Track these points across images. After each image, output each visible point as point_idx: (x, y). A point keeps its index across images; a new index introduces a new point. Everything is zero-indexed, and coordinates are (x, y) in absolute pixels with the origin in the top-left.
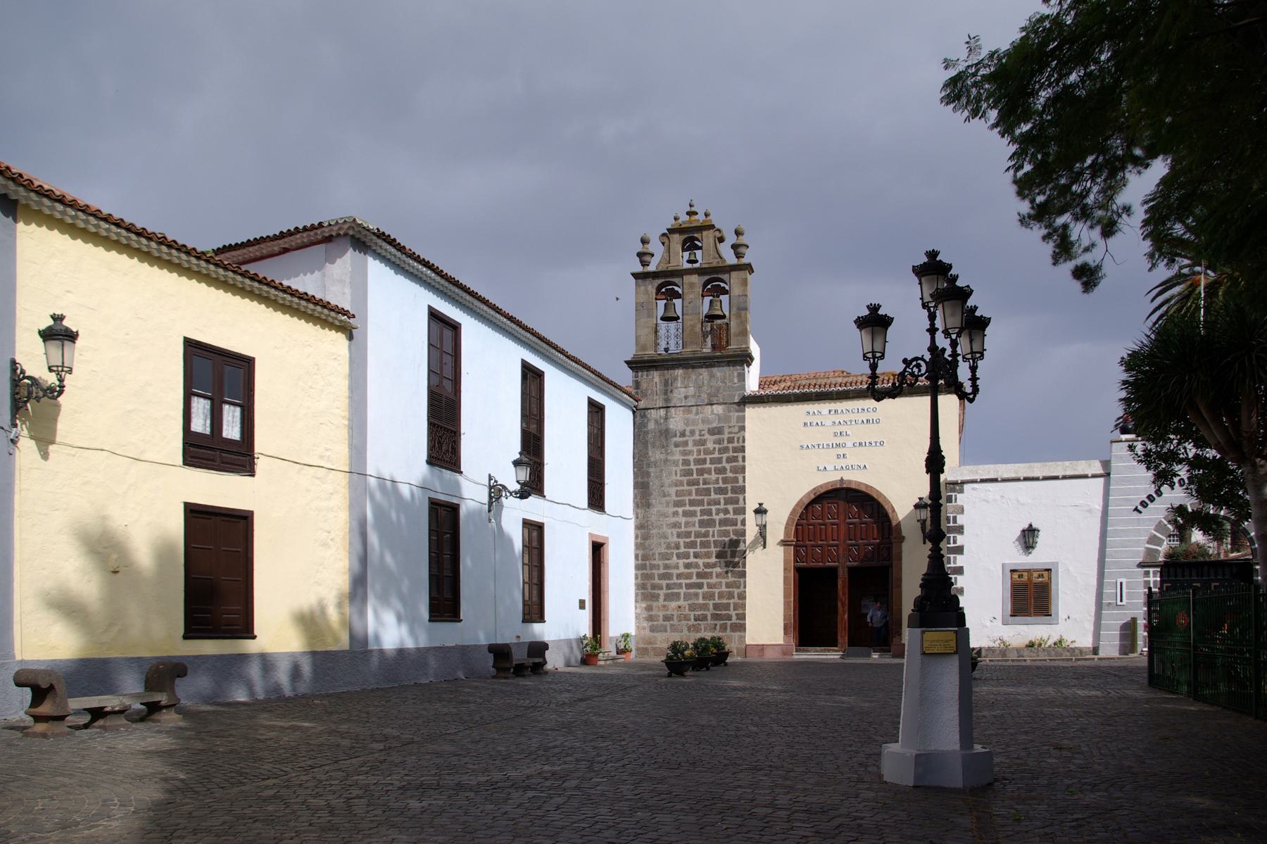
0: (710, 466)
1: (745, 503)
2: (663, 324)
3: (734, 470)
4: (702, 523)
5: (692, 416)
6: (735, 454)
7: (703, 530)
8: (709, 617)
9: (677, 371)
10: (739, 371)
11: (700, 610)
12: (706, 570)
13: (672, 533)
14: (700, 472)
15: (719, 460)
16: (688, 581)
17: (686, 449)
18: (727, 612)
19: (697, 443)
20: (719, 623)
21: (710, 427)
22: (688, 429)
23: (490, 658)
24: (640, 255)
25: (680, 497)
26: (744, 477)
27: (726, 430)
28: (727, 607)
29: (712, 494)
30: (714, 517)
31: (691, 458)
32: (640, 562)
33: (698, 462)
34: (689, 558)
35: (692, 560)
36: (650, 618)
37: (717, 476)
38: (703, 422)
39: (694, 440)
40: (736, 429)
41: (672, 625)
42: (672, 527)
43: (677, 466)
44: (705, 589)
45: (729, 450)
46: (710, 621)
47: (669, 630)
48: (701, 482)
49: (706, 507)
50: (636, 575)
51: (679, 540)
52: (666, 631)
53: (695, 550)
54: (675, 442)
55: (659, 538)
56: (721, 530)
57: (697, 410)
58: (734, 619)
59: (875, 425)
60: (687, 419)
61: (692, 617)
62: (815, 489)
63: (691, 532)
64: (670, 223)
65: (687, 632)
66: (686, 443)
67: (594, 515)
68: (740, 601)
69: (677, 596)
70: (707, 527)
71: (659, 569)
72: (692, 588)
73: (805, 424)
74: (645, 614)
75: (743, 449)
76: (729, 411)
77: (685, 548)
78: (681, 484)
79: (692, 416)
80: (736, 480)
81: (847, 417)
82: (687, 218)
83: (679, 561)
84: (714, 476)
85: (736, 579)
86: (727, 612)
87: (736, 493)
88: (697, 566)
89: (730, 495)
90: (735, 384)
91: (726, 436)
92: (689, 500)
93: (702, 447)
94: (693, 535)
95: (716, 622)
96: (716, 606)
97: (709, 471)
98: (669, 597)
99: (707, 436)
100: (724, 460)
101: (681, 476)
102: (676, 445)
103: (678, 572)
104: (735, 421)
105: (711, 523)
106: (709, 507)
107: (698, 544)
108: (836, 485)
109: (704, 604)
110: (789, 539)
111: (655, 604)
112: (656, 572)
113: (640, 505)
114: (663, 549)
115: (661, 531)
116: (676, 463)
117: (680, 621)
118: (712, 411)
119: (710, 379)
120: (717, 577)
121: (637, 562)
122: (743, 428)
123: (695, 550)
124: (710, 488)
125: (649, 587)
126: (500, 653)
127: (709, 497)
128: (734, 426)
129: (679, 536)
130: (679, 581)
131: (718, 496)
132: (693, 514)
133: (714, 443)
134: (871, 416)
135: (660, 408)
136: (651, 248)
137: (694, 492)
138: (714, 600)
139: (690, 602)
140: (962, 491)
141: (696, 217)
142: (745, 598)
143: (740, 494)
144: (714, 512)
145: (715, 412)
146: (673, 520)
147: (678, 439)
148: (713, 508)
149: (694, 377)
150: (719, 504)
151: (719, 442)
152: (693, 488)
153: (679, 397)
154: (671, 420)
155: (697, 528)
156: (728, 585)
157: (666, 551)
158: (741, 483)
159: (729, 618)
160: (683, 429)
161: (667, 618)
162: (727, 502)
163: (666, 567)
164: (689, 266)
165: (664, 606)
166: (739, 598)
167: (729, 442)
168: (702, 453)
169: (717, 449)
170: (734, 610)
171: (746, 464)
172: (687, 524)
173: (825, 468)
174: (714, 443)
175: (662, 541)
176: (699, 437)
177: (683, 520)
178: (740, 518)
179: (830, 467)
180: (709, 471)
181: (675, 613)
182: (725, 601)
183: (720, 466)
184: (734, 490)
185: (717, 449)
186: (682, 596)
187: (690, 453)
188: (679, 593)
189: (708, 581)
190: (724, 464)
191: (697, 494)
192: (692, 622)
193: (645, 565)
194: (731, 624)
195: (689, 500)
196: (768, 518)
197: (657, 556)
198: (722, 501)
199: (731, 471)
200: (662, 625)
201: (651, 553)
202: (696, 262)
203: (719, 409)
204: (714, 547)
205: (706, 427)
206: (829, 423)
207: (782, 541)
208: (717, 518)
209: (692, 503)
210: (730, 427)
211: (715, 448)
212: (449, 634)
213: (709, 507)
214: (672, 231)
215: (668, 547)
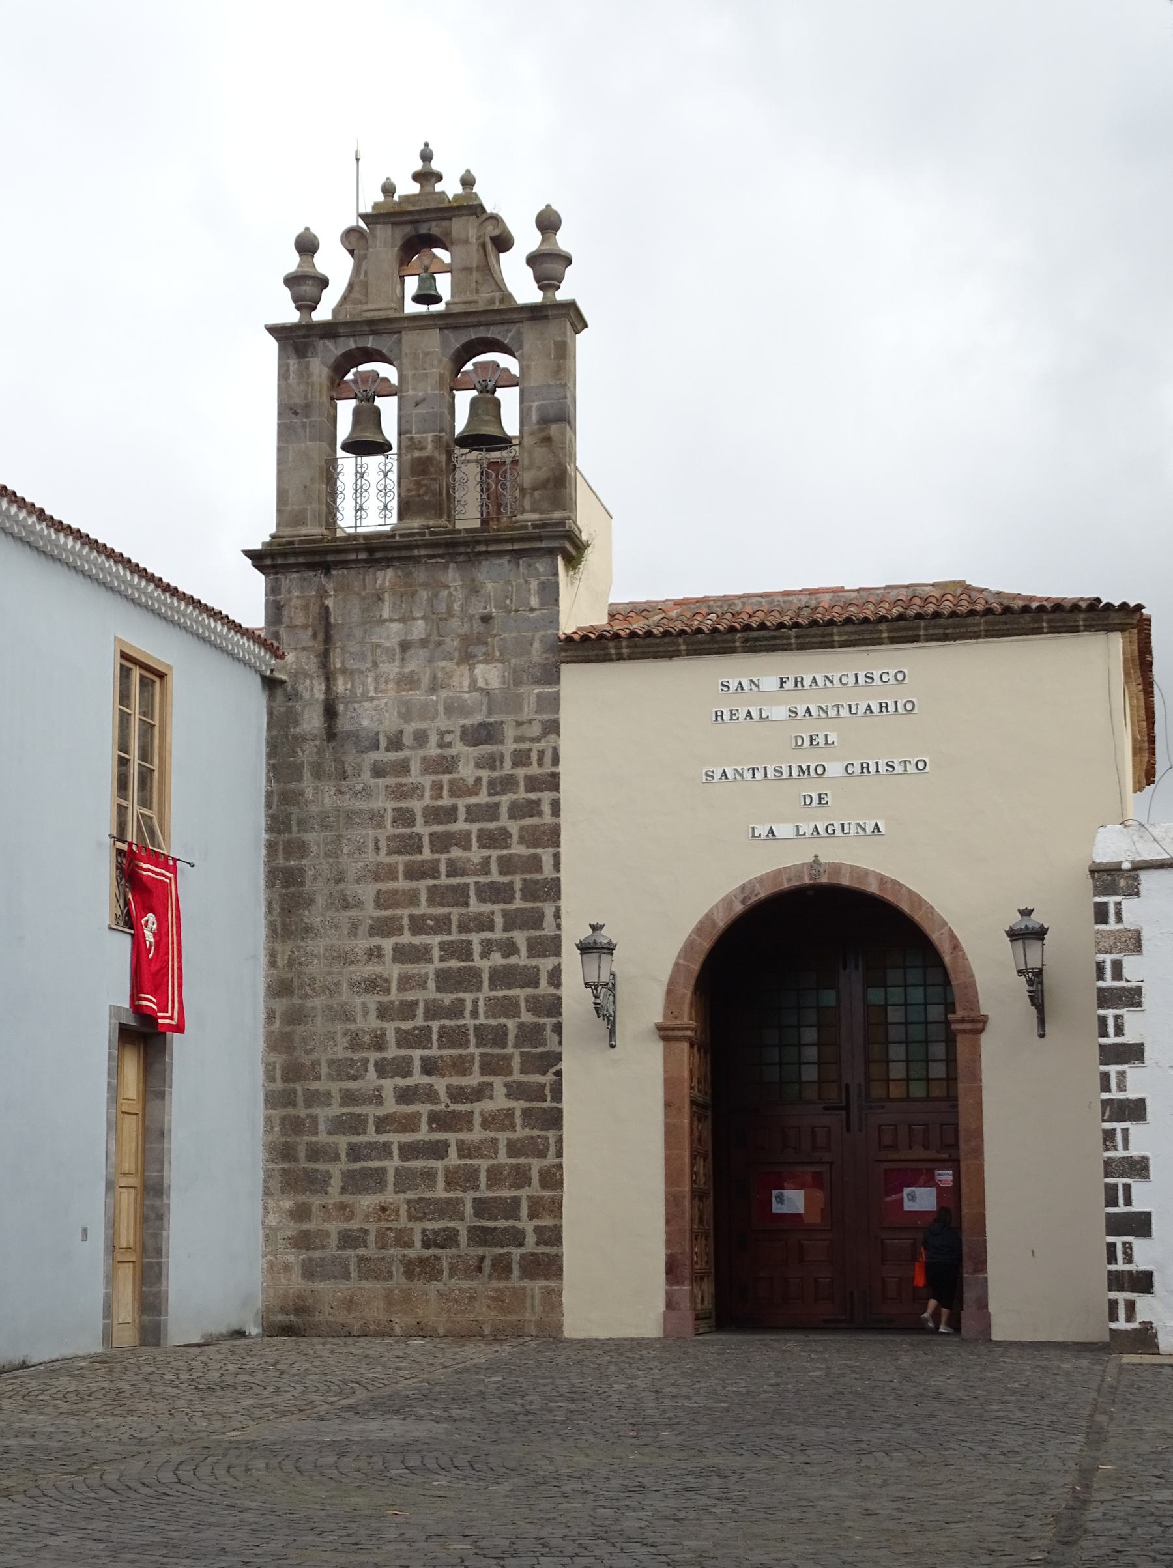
0: (467, 826)
1: (559, 926)
2: (347, 463)
3: (534, 838)
4: (445, 980)
5: (417, 696)
6: (533, 796)
7: (448, 999)
8: (463, 1238)
9: (380, 574)
10: (543, 578)
11: (440, 1218)
12: (453, 1107)
13: (364, 1005)
14: (442, 843)
15: (491, 812)
16: (407, 1138)
17: (403, 780)
18: (511, 1223)
20: (491, 1252)
21: (468, 722)
22: (409, 729)
24: (291, 281)
25: (386, 909)
26: (557, 858)
27: (510, 732)
28: (510, 1209)
29: (473, 900)
30: (478, 962)
31: (417, 806)
32: (279, 1085)
33: (436, 815)
34: (407, 1074)
35: (418, 1078)
36: (303, 1241)
37: (486, 853)
38: (450, 709)
39: (424, 759)
40: (536, 730)
41: (362, 1259)
42: (367, 991)
43: (380, 825)
44: (453, 1159)
45: (516, 784)
46: (465, 1249)
47: (354, 1274)
48: (443, 868)
49: (455, 936)
50: (268, 1120)
51: (385, 1025)
52: (347, 1277)
53: (426, 1053)
54: (376, 761)
55: (332, 1021)
56: (497, 998)
60: (406, 703)
61: (418, 1238)
62: (743, 887)
63: (417, 1002)
65: (403, 1280)
66: (403, 767)
68: (547, 1194)
70: (458, 991)
71: (329, 1105)
72: (417, 1158)
74: (291, 1229)
75: (553, 782)
76: (518, 682)
77: (399, 1045)
78: (391, 874)
79: (417, 696)
80: (535, 864)
82: (415, 188)
83: (382, 1082)
84: (476, 854)
85: (536, 1133)
86: (511, 1223)
87: (535, 899)
88: (430, 1095)
89: (518, 904)
90: (532, 610)
91: (509, 747)
92: (411, 917)
93: (446, 778)
94: (420, 1011)
95: (480, 1251)
96: (482, 1207)
97: (463, 841)
98: (356, 1182)
99: (458, 748)
100: (504, 810)
101: (389, 853)
102: (379, 771)
103: (381, 1111)
104: (533, 705)
105: (467, 980)
106: (464, 937)
107: (435, 1037)
108: (800, 877)
109: (449, 1201)
110: (677, 1022)
111: (316, 1201)
113: (279, 930)
114: (340, 1048)
115: (334, 1002)
116: (376, 819)
117: (383, 1247)
118: (473, 682)
119: (467, 599)
120: (485, 1125)
121: (273, 1086)
122: (553, 727)
123: (426, 1053)
124: (468, 885)
125: (302, 1155)
127: (464, 910)
128: (530, 722)
129: (384, 1013)
130: (383, 1138)
131: (486, 908)
132: (420, 954)
133: (478, 766)
137: (424, 897)
138: (476, 1188)
139: (410, 1195)
140: (1135, 893)
141: (439, 187)
142: (560, 1184)
143: (545, 901)
144: (477, 949)
145: (481, 684)
146: (366, 970)
147: (383, 756)
148: (476, 938)
149: (424, 594)
150: (491, 928)
151: (491, 762)
152: (423, 885)
153: (388, 644)
154: (366, 704)
155: (431, 993)
156: (514, 1149)
157: (349, 1054)
158: (548, 872)
159: (518, 1238)
160: (394, 729)
161: (350, 1240)
163: (349, 1098)
164: (422, 309)
165: (342, 1207)
166: (544, 1185)
167: (515, 764)
168: (445, 793)
169: (485, 783)
170: (532, 1216)
171: (565, 819)
172: (405, 982)
173: (771, 831)
174: (478, 766)
175: (339, 1027)
176: (439, 751)
177: (394, 971)
178: (547, 964)
179: (784, 830)
180: (463, 841)
181: (372, 1227)
182: (506, 1193)
183: (492, 826)
185: (485, 783)
186: (391, 1178)
188: (383, 1172)
189: (462, 1136)
190: (505, 821)
191: (431, 902)
192: (417, 1251)
194: (523, 1256)
195: (411, 917)
196: (619, 962)
197: (324, 1070)
198: (499, 921)
199: (522, 840)
200: (334, 1259)
202: (437, 299)
203: (489, 675)
204: (478, 1046)
205: (457, 723)
206: (779, 712)
207: (660, 1028)
208: (483, 965)
209: (418, 926)
210: (519, 724)
211: (478, 780)
213: (464, 937)
215: (355, 1044)
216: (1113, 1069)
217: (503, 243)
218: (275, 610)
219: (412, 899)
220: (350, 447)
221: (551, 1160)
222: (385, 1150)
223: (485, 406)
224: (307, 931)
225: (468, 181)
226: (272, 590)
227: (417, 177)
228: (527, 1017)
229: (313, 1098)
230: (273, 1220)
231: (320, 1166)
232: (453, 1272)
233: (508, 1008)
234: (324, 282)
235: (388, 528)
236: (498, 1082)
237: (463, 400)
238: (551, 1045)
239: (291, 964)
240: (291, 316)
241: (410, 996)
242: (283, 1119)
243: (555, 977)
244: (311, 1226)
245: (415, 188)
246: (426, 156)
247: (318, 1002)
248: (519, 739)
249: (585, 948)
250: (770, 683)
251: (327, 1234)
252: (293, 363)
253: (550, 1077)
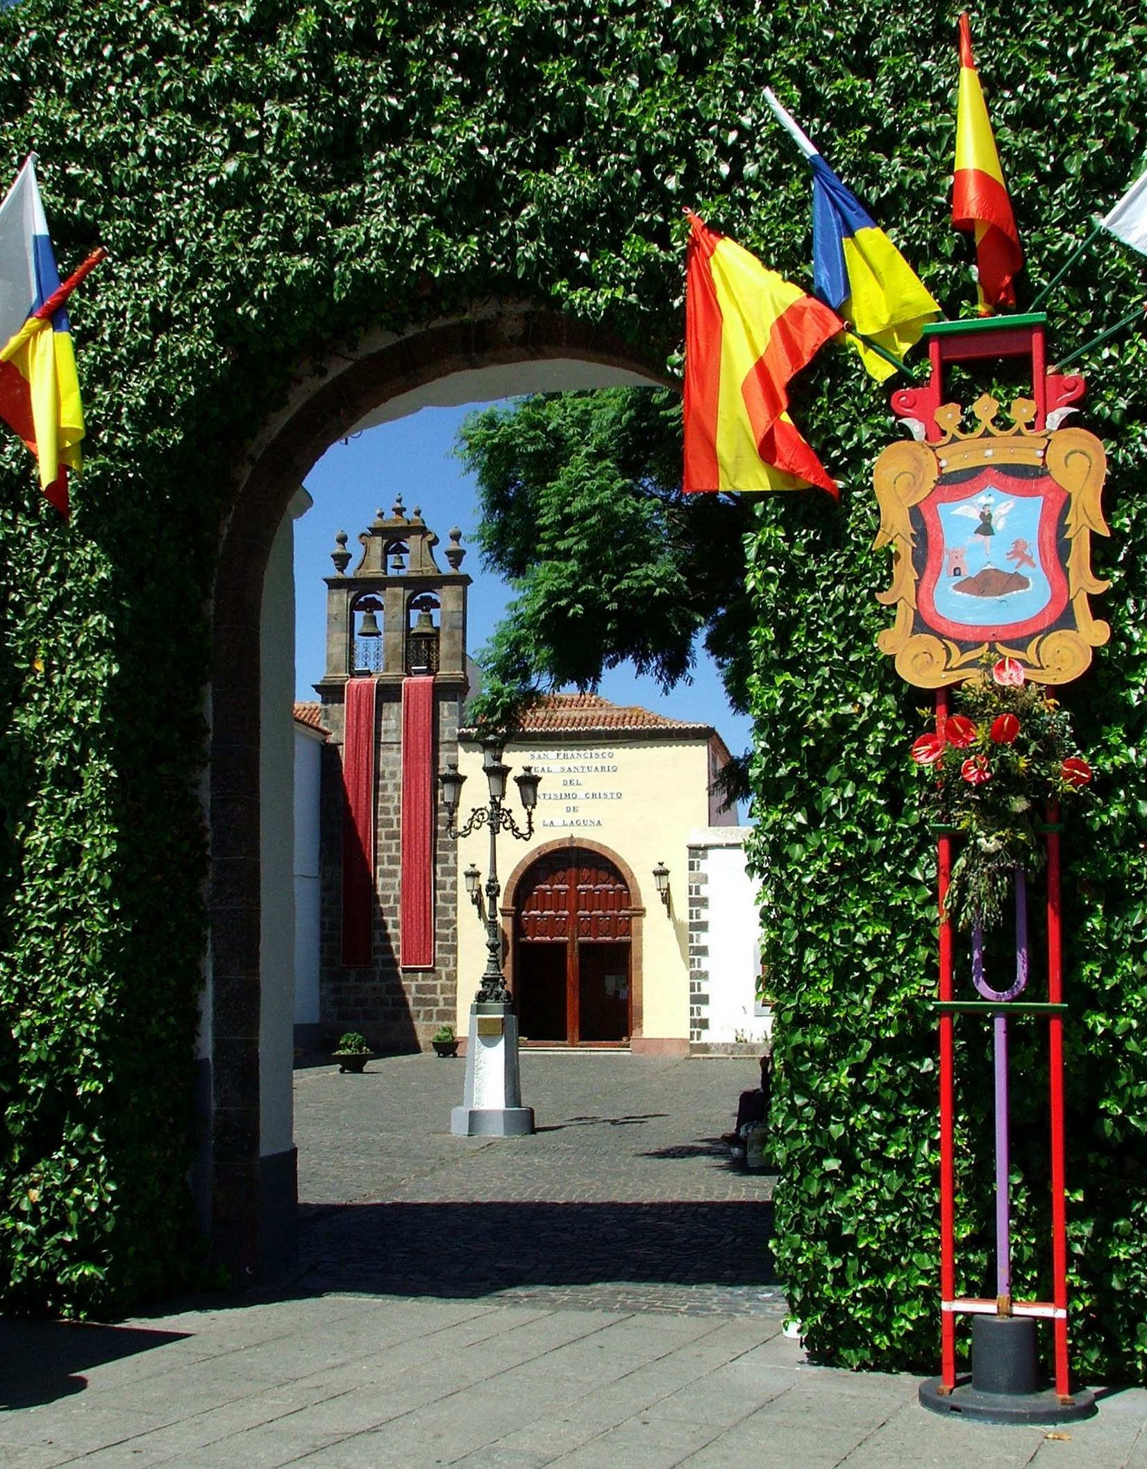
28: (432, 989)
32: (326, 932)
58: (441, 1006)
59: (611, 774)
64: (374, 521)
82: (394, 516)
134: (607, 762)
178: (451, 879)
179: (558, 822)
214: (375, 531)
216: (694, 933)
221: (451, 968)
225: (418, 513)
238: (452, 916)
241: (388, 893)
243: (454, 886)
249: (467, 875)
253: (451, 931)
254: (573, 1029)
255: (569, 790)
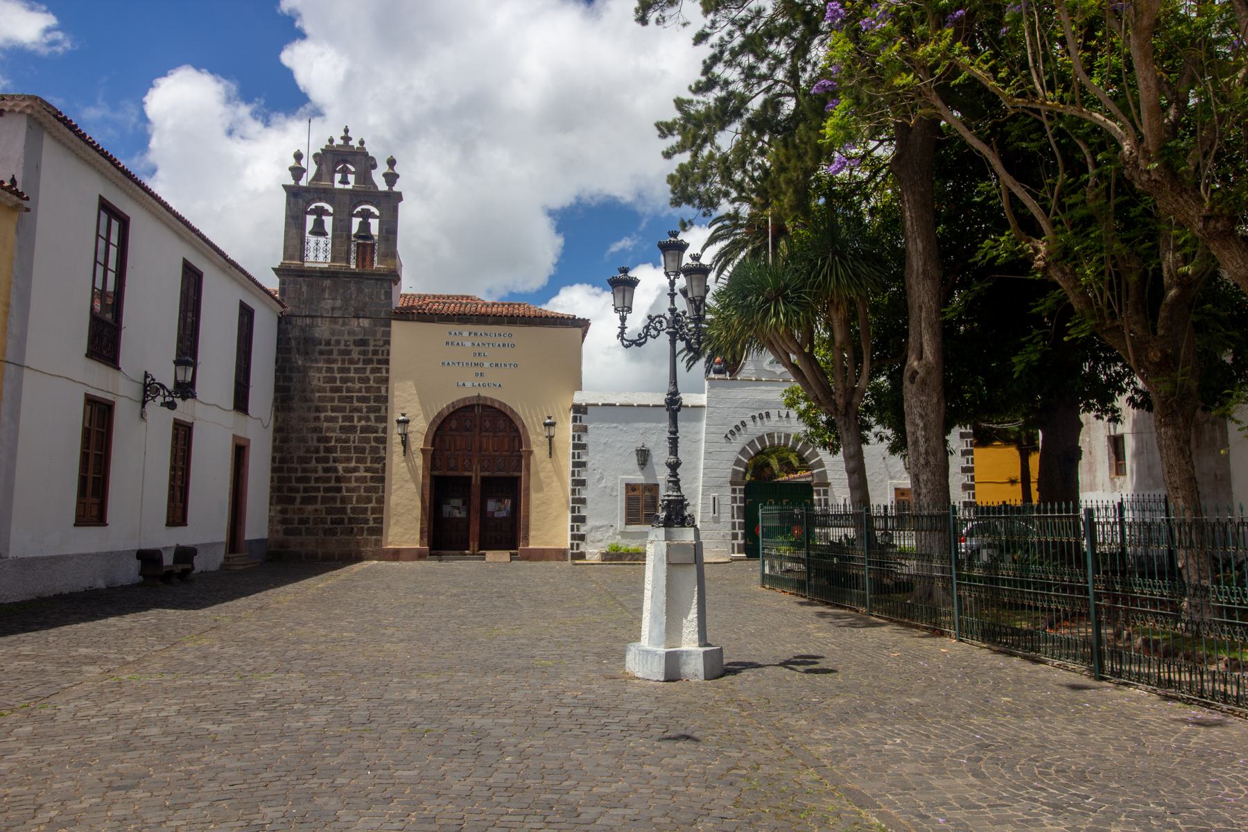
5: (338, 327)
7: (344, 436)
14: (344, 380)
16: (326, 485)
19: (341, 353)
22: (334, 338)
23: (135, 566)
26: (387, 388)
27: (372, 343)
28: (365, 510)
32: (277, 465)
33: (341, 370)
34: (328, 462)
36: (284, 521)
40: (381, 343)
41: (307, 528)
43: (320, 372)
57: (344, 322)
58: (371, 524)
66: (331, 352)
67: (240, 417)
69: (313, 500)
73: (447, 343)
74: (280, 517)
75: (387, 362)
76: (376, 326)
79: (338, 327)
80: (379, 389)
81: (486, 340)
82: (341, 142)
84: (358, 385)
89: (372, 404)
91: (371, 348)
97: (352, 380)
98: (305, 501)
99: (352, 347)
102: (321, 353)
103: (317, 475)
105: (352, 429)
111: (290, 507)
112: (293, 475)
122: (388, 343)
125: (285, 489)
126: (149, 558)
131: (360, 404)
133: (359, 354)
134: (507, 341)
135: (306, 316)
136: (304, 163)
139: (327, 506)
141: (351, 143)
146: (313, 425)
147: (323, 347)
148: (356, 415)
152: (336, 395)
156: (367, 490)
161: (302, 521)
162: (370, 410)
163: (304, 470)
164: (341, 186)
165: (300, 509)
166: (377, 502)
175: (302, 445)
179: (468, 384)
180: (352, 380)
181: (311, 517)
184: (377, 399)
187: (334, 361)
188: (317, 497)
189: (348, 485)
191: (339, 401)
193: (283, 468)
196: (411, 427)
201: (289, 456)
202: (348, 183)
203: (365, 323)
205: (352, 338)
206: (468, 344)
209: (333, 410)
212: (91, 540)
215: (308, 451)
217: (374, 166)
218: (283, 291)
219: (332, 399)
220: (312, 233)
221: (380, 494)
222: (318, 490)
223: (365, 226)
224: (290, 409)
225: (362, 143)
226: (282, 283)
227: (342, 138)
228: (373, 444)
229: (290, 470)
230: (273, 514)
231: (293, 495)
232: (342, 533)
233: (367, 440)
234: (304, 170)
235: (326, 266)
236: (362, 466)
237: (356, 222)
238: (382, 454)
239: (284, 420)
240: (291, 182)
242: (278, 477)
244: (288, 516)
245: (341, 142)
246: (346, 131)
247: (294, 435)
248: (375, 346)
250: (466, 334)
251: (294, 519)
252: (292, 199)
253: (381, 465)
254: (474, 545)
255: (477, 360)
